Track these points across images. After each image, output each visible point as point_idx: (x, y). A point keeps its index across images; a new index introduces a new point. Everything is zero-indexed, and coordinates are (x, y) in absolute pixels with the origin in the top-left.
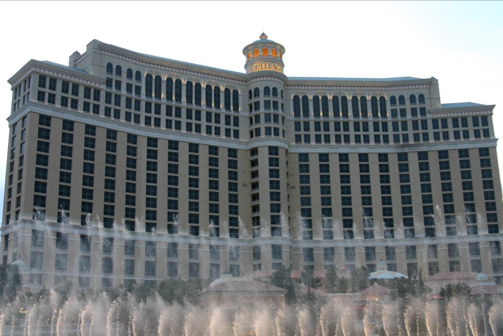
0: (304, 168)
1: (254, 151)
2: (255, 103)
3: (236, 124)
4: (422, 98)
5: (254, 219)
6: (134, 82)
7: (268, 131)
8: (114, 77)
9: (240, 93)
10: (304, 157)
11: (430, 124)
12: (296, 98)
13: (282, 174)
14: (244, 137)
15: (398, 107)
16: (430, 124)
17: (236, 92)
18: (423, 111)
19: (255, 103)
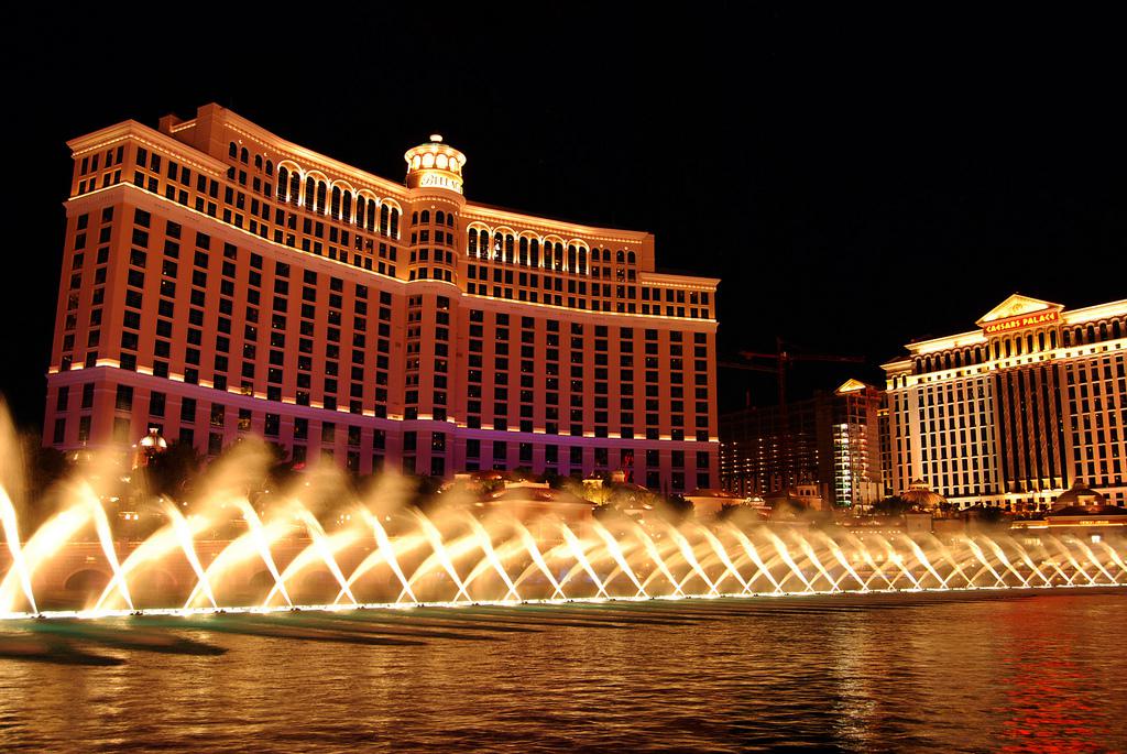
0: (476, 331)
1: (416, 300)
2: (422, 232)
3: (393, 258)
4: (632, 257)
5: (408, 393)
6: (264, 179)
7: (437, 275)
8: (239, 166)
9: (400, 213)
10: (477, 315)
11: (639, 294)
13: (451, 335)
14: (402, 279)
15: (602, 264)
16: (639, 294)
18: (632, 274)
19: (422, 232)
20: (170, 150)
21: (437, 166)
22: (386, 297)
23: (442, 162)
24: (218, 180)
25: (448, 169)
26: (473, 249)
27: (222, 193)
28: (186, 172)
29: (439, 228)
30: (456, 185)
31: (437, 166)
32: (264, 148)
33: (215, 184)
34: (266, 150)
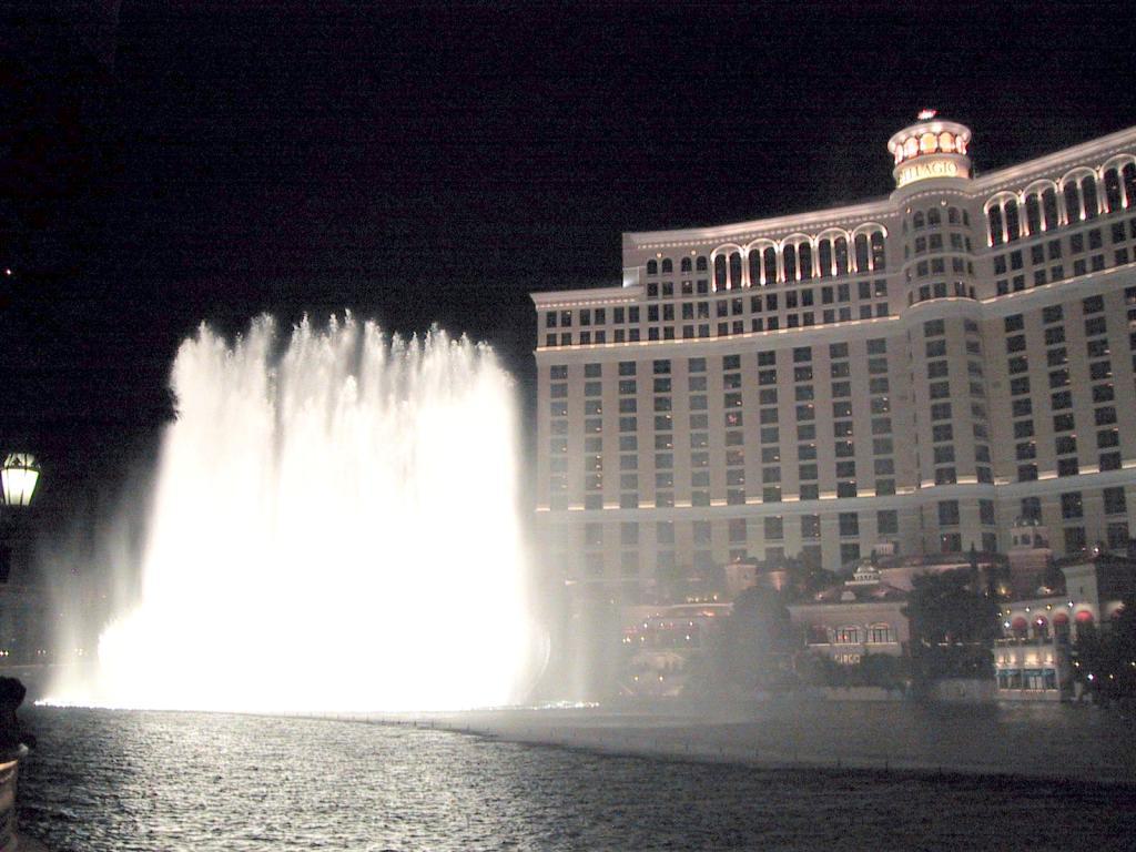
8: (660, 279)
9: (885, 234)
12: (994, 210)
17: (877, 237)
20: (577, 301)
21: (929, 151)
22: (876, 345)
23: (911, 149)
24: (636, 304)
25: (919, 153)
26: (997, 236)
27: (643, 314)
28: (600, 314)
29: (921, 233)
30: (949, 170)
31: (929, 151)
32: (935, 197)
33: (634, 312)
34: (693, 248)
